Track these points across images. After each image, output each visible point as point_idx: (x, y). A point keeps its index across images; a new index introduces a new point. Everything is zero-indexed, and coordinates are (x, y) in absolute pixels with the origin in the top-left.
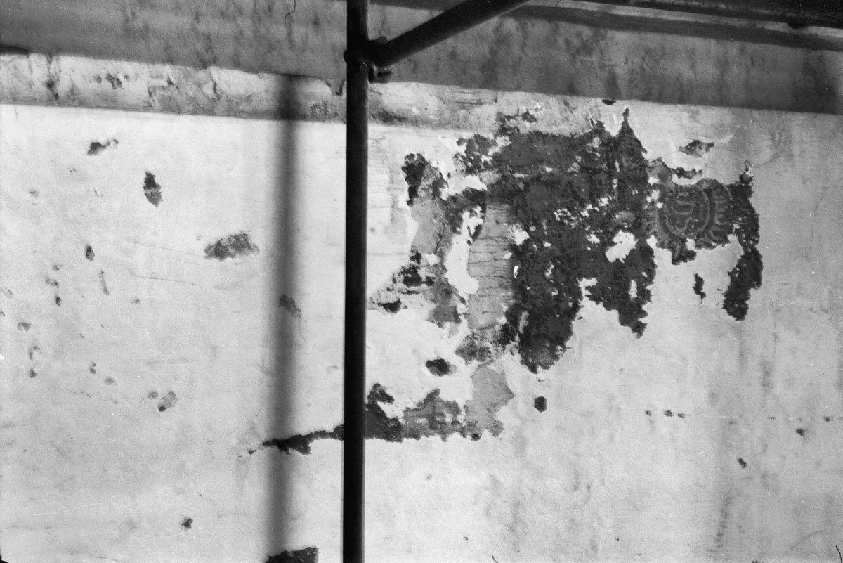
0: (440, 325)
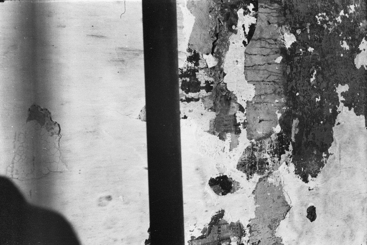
0: (222, 138)
